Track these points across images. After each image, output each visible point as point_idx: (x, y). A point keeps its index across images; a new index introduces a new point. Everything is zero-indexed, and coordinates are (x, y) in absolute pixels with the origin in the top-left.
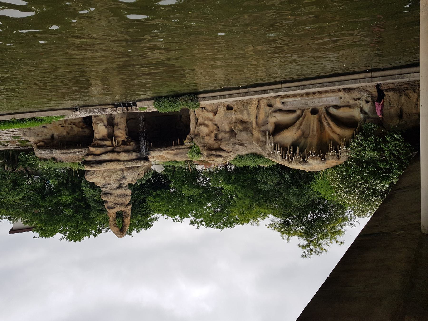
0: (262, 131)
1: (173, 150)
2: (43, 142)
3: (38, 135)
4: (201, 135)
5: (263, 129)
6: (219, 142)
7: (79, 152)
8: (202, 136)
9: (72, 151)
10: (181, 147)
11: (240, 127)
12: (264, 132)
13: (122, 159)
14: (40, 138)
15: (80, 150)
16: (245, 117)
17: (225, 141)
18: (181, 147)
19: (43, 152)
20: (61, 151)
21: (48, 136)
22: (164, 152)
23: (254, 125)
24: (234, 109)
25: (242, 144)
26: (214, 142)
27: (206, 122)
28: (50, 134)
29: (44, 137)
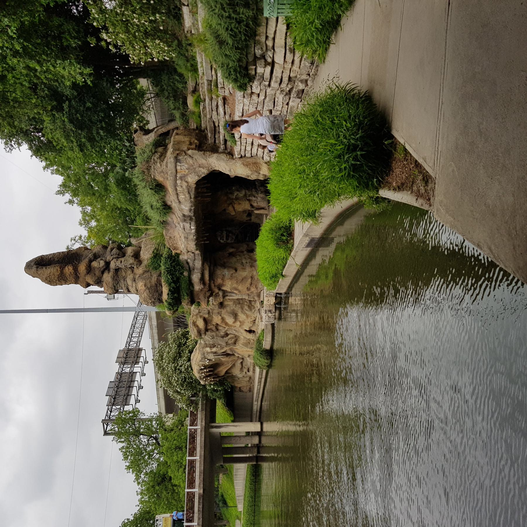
4: (222, 310)
6: (214, 329)
8: (221, 311)
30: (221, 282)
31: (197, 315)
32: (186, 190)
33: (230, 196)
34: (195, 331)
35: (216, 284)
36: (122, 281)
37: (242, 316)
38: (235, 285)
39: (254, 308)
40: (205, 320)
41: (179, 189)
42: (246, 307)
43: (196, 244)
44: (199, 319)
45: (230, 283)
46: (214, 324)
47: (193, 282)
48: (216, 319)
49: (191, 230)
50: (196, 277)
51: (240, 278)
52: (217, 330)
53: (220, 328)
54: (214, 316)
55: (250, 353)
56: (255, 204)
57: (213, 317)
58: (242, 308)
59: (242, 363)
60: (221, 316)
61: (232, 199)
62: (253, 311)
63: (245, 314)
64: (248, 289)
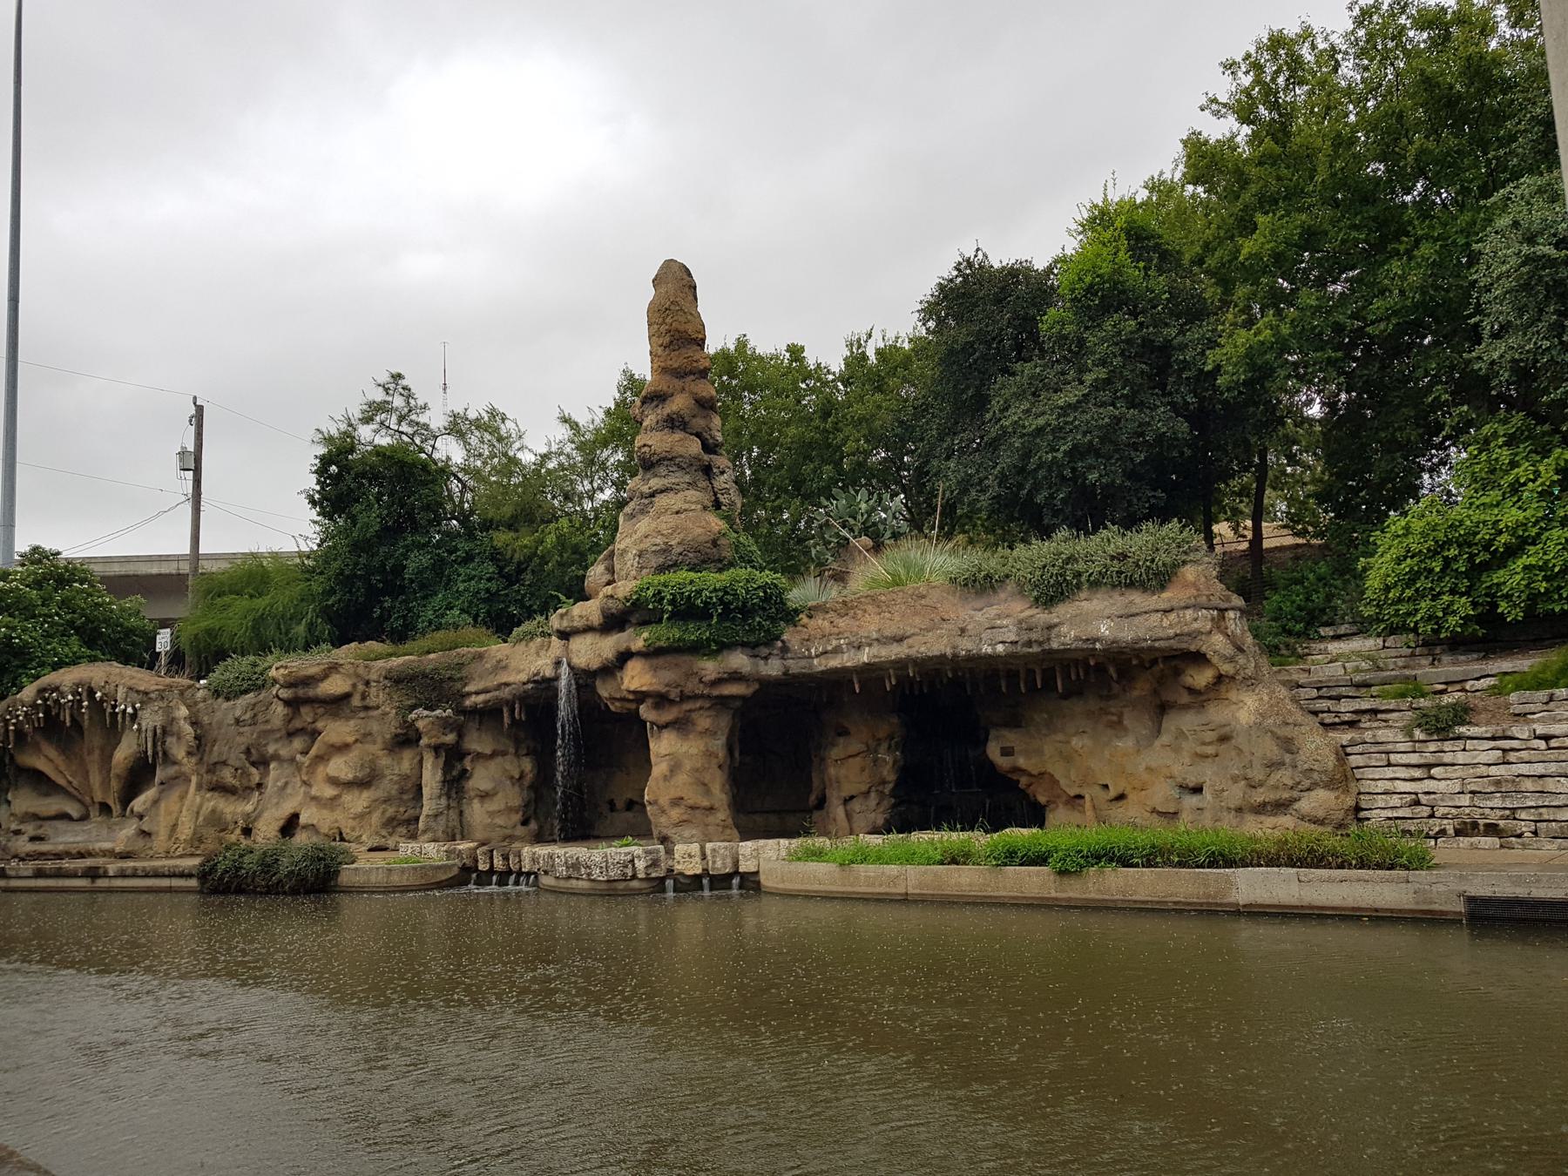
0: (175, 763)
1: (507, 684)
2: (1191, 690)
3: (1224, 739)
4: (379, 745)
5: (172, 771)
6: (297, 724)
7: (837, 650)
8: (374, 743)
9: (865, 656)
10: (488, 696)
11: (227, 776)
12: (168, 759)
13: (589, 639)
14: (1217, 714)
15: (835, 663)
17: (272, 731)
18: (488, 696)
19: (1104, 629)
20: (913, 652)
21: (1172, 722)
22: (523, 677)
23: (194, 779)
24: (238, 831)
25: (237, 721)
26: (319, 725)
27: (330, 792)
28: (1157, 743)
29: (1187, 721)
30: (699, 728)
31: (358, 676)
32: (1186, 629)
33: (885, 746)
34: (312, 671)
35: (694, 716)
36: (687, 478)
37: (358, 801)
38: (688, 765)
39: (391, 834)
40: (347, 696)
41: (1189, 614)
42: (391, 811)
43: (944, 656)
45: (694, 751)
46: (319, 725)
47: (725, 653)
48: (336, 730)
50: (739, 660)
51: (707, 778)
52: (291, 735)
53: (298, 743)
54: (352, 723)
55: (160, 842)
56: (856, 805)
57: (348, 719)
59: (64, 816)
60: (356, 741)
61: (876, 752)
62: (384, 833)
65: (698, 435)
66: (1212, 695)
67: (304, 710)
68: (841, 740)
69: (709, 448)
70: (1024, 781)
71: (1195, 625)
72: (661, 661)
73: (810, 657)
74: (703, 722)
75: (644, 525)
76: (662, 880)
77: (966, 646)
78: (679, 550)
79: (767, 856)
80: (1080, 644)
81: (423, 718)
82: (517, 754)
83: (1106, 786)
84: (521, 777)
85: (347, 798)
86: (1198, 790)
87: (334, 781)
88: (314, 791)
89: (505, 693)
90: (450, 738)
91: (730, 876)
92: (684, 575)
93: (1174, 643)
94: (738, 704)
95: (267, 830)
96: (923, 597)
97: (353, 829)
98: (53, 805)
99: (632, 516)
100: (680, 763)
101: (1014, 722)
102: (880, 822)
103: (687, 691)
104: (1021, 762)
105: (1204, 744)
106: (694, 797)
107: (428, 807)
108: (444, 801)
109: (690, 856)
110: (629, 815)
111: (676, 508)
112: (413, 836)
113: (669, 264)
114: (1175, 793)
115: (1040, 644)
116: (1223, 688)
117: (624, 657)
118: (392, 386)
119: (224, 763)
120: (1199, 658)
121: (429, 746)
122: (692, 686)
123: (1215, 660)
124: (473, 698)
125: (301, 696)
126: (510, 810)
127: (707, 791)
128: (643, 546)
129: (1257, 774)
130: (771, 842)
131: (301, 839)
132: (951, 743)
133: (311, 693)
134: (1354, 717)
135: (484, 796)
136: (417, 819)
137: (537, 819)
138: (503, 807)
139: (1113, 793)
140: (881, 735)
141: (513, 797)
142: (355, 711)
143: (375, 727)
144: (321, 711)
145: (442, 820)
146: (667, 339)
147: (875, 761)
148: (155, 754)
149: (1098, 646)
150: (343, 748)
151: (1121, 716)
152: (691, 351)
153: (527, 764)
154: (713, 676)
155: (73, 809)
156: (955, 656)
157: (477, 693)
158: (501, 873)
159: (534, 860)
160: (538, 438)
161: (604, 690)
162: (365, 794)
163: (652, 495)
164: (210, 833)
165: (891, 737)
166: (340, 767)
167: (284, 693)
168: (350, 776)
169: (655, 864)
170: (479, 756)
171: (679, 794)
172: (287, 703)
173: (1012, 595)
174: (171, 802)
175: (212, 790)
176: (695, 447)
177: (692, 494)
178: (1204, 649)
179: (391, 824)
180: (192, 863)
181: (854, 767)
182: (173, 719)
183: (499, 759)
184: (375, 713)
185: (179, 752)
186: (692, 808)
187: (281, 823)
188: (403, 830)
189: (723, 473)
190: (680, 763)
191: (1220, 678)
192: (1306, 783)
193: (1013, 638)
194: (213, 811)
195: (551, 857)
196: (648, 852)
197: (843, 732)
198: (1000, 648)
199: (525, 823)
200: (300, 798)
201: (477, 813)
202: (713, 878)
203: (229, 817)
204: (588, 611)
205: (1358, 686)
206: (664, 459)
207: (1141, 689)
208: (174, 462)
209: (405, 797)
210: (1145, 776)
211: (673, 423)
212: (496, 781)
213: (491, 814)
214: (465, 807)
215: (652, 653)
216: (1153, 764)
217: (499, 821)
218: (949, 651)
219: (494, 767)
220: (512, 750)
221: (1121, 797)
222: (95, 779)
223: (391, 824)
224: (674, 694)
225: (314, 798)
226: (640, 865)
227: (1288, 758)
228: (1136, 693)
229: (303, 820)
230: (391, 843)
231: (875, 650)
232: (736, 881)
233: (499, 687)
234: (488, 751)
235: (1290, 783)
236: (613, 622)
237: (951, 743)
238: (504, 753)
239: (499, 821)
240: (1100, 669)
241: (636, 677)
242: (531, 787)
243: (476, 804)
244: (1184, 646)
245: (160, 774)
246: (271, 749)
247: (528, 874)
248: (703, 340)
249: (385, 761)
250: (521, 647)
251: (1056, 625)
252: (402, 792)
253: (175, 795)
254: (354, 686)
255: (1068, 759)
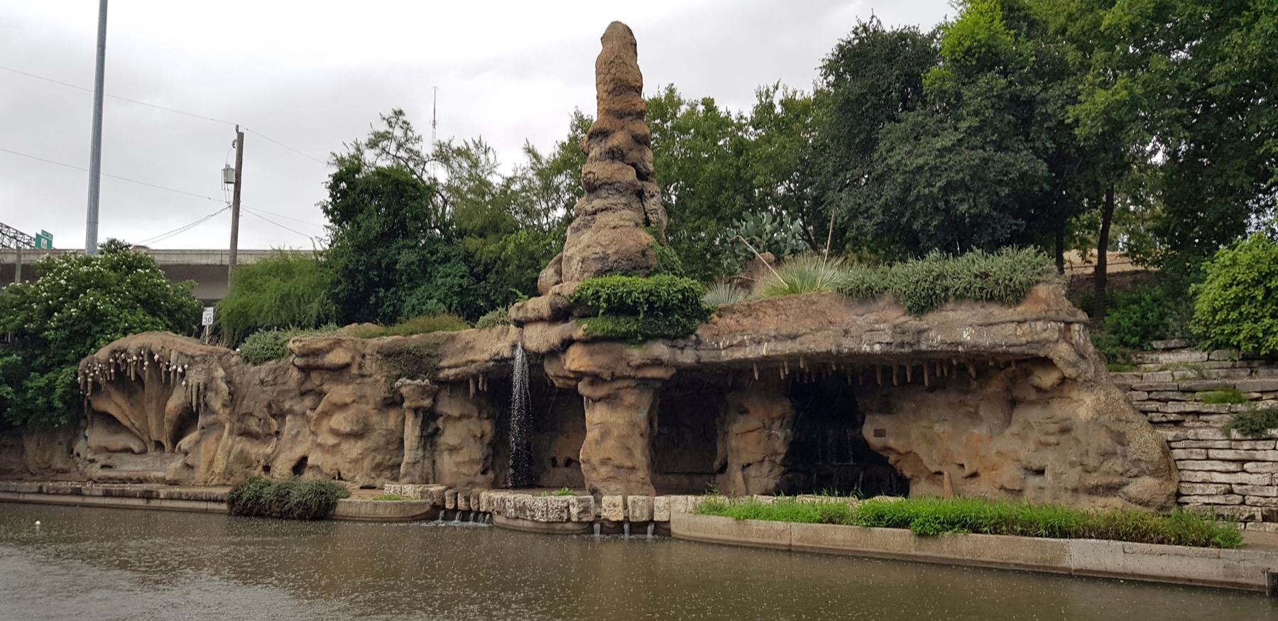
0: (213, 412)
1: (473, 362)
2: (1039, 389)
3: (1065, 431)
5: (211, 418)
6: (308, 386)
7: (741, 344)
8: (368, 403)
9: (764, 350)
10: (458, 370)
11: (253, 425)
12: (208, 409)
14: (1059, 409)
15: (739, 354)
16: (242, 444)
17: (288, 391)
18: (458, 370)
19: (966, 336)
20: (804, 348)
21: (1020, 415)
22: (486, 356)
23: (227, 426)
24: (260, 468)
25: (262, 382)
26: (325, 387)
27: (332, 440)
28: (1007, 432)
29: (1034, 415)
31: (356, 350)
32: (1036, 338)
33: (778, 424)
34: (321, 344)
36: (623, 200)
37: (354, 449)
38: (615, 432)
41: (1040, 325)
42: (379, 458)
43: (829, 352)
44: (350, 355)
45: (621, 421)
48: (338, 392)
49: (871, 345)
50: (660, 349)
51: (631, 444)
52: (303, 394)
53: (308, 401)
54: (351, 387)
56: (752, 471)
57: (348, 384)
58: (375, 450)
59: (128, 450)
61: (770, 429)
63: (363, 456)
64: (605, 462)
65: (634, 165)
66: (1056, 394)
67: (314, 375)
68: (742, 418)
69: (642, 176)
70: (892, 458)
71: (1045, 335)
72: (596, 347)
73: (718, 349)
74: (630, 398)
75: (586, 237)
76: (591, 524)
77: (848, 345)
78: (615, 258)
79: (677, 509)
80: (945, 347)
81: (406, 386)
82: (479, 417)
83: (962, 466)
84: (482, 436)
85: (345, 446)
86: (1040, 472)
87: (335, 433)
88: (319, 440)
89: (472, 368)
90: (427, 402)
91: (646, 524)
92: (617, 279)
93: (1026, 350)
94: (659, 385)
95: (282, 469)
96: (814, 303)
97: (349, 471)
98: (120, 441)
99: (577, 230)
100: (610, 430)
101: (887, 408)
102: (772, 485)
103: (617, 373)
104: (891, 442)
105: (1047, 434)
106: (619, 458)
107: (408, 456)
108: (420, 452)
109: (614, 506)
110: (567, 470)
111: (613, 224)
112: (395, 479)
113: (615, 25)
114: (1021, 474)
115: (911, 345)
116: (1066, 388)
117: (567, 343)
118: (393, 120)
119: (251, 415)
120: (1047, 363)
121: (409, 408)
122: (621, 369)
123: (1060, 364)
124: (446, 372)
125: (311, 365)
126: (472, 462)
127: (631, 455)
128: (585, 254)
129: (1092, 462)
130: (680, 497)
131: (308, 476)
132: (834, 424)
133: (319, 362)
134: (1180, 418)
135: (453, 450)
136: (399, 465)
137: (493, 469)
138: (467, 459)
139: (968, 471)
140: (775, 415)
141: (475, 451)
142: (352, 379)
143: (368, 391)
144: (326, 376)
145: (419, 467)
146: (612, 86)
147: (769, 436)
148: (198, 405)
149: (960, 349)
150: (344, 406)
151: (977, 407)
152: (630, 96)
153: (487, 426)
154: (638, 362)
155: (135, 445)
156: (839, 352)
157: (449, 368)
158: (463, 512)
159: (490, 502)
160: (507, 165)
161: (550, 369)
162: (360, 444)
163: (595, 213)
164: (239, 469)
165: (783, 417)
166: (339, 421)
167: (299, 362)
168: (348, 429)
169: (585, 510)
170: (449, 417)
171: (607, 455)
172: (301, 369)
173: (889, 304)
174: (209, 443)
175: (241, 435)
176: (631, 175)
177: (627, 213)
178: (1051, 355)
179: (379, 468)
180: (223, 491)
181: (753, 438)
182: (213, 378)
183: (465, 421)
184: (368, 380)
185: (217, 404)
186: (619, 467)
187: (293, 463)
188: (387, 473)
189: (652, 196)
190: (610, 431)
191: (1064, 380)
192: (1135, 471)
193: (888, 340)
194: (242, 451)
195: (503, 500)
196: (580, 501)
197: (745, 412)
198: (877, 348)
199: (484, 472)
200: (308, 444)
201: (447, 463)
202: (632, 524)
203: (253, 457)
204: (539, 305)
205: (1184, 391)
206: (605, 184)
207: (996, 386)
208: (220, 177)
209: (391, 447)
210: (996, 459)
211: (614, 155)
212: (463, 437)
213: (458, 464)
214: (437, 457)
215: (589, 341)
216: (1004, 450)
217: (464, 470)
218: (834, 349)
219: (462, 427)
220: (476, 414)
221: (974, 475)
222: (153, 423)
223: (379, 468)
224: (606, 375)
225: (319, 445)
226: (574, 510)
227: (1119, 449)
228: (990, 390)
229: (310, 462)
230: (378, 483)
231: (772, 345)
232: (650, 528)
233: (466, 363)
234: (456, 413)
235: (1121, 470)
236: (559, 315)
237: (834, 424)
238: (469, 417)
239: (464, 470)
240: (962, 368)
241: (576, 360)
242: (490, 444)
243: (446, 456)
244: (1033, 351)
245: (202, 420)
246: (287, 405)
247: (485, 513)
248: (641, 88)
249: (375, 418)
250: (486, 332)
251: (925, 331)
252: (388, 443)
253: (212, 438)
254: (353, 358)
255: (931, 442)
